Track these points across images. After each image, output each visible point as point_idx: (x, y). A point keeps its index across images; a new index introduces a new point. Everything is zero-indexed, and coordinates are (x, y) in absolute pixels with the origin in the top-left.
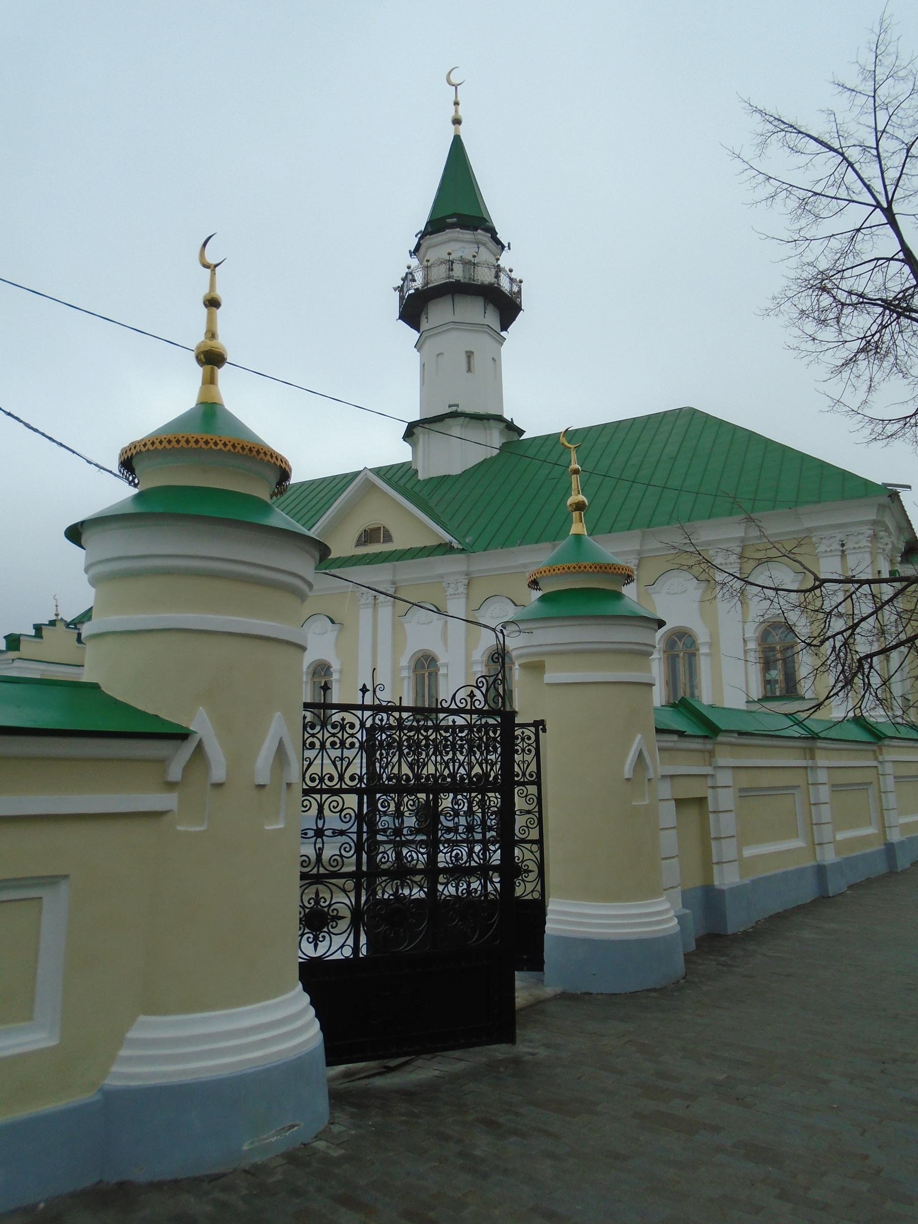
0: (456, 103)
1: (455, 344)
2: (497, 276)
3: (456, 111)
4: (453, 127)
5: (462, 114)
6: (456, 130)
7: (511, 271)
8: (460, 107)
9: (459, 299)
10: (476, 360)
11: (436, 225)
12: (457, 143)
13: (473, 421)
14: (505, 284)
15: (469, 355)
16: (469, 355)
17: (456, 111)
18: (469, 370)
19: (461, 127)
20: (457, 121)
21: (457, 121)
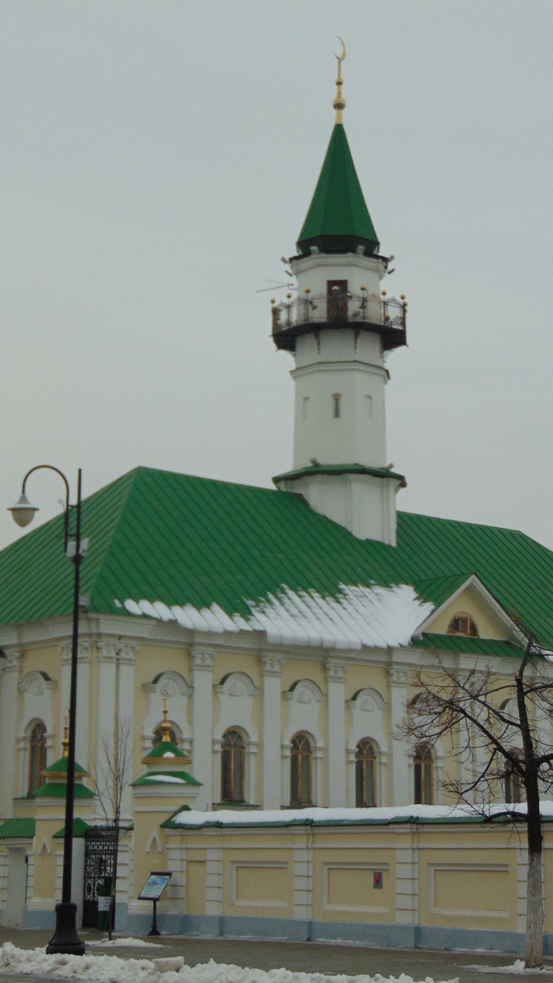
0: (339, 83)
1: (323, 384)
2: (363, 307)
3: (339, 93)
4: (334, 112)
5: (346, 98)
6: (339, 116)
7: (384, 294)
8: (343, 87)
9: (325, 336)
10: (343, 403)
11: (305, 245)
12: (339, 134)
13: (333, 478)
14: (374, 315)
15: (337, 398)
16: (337, 398)
17: (339, 93)
18: (337, 414)
19: (344, 112)
20: (339, 106)
21: (339, 106)
